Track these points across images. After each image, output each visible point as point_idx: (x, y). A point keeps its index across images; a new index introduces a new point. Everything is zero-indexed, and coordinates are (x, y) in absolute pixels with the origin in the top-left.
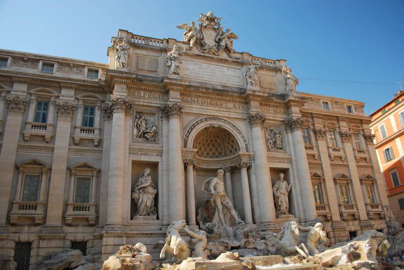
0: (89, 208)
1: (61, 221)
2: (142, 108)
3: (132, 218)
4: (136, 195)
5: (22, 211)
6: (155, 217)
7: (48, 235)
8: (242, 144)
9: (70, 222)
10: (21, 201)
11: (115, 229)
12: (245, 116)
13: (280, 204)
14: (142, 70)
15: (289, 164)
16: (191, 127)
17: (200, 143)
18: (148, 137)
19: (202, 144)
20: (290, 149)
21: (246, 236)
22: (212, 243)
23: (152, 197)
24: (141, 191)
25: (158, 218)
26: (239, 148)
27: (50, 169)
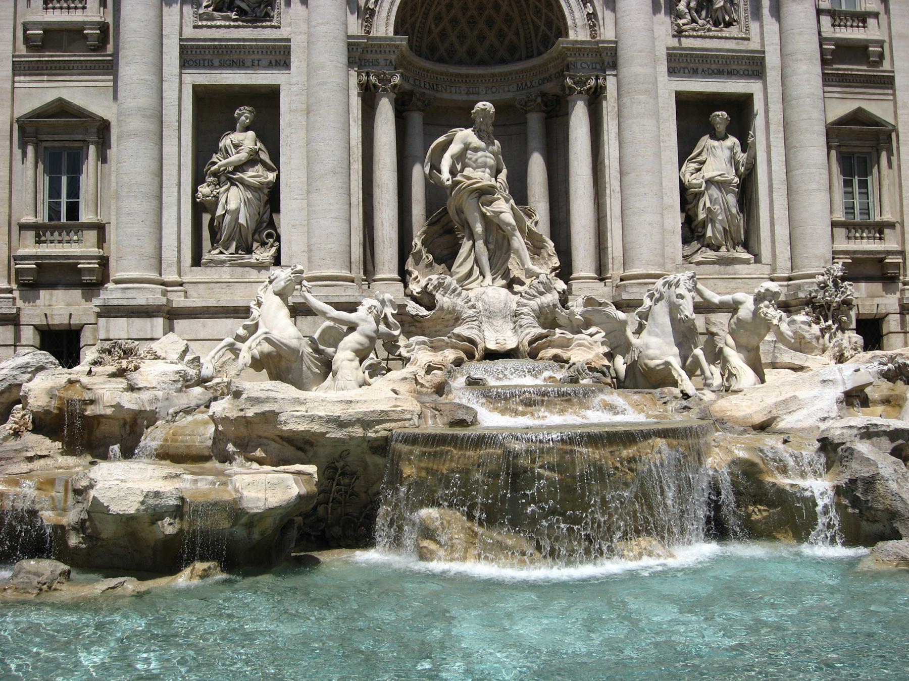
3: (197, 261)
11: (130, 294)
13: (702, 215)
17: (438, 18)
21: (548, 319)
24: (223, 178)
26: (566, 28)
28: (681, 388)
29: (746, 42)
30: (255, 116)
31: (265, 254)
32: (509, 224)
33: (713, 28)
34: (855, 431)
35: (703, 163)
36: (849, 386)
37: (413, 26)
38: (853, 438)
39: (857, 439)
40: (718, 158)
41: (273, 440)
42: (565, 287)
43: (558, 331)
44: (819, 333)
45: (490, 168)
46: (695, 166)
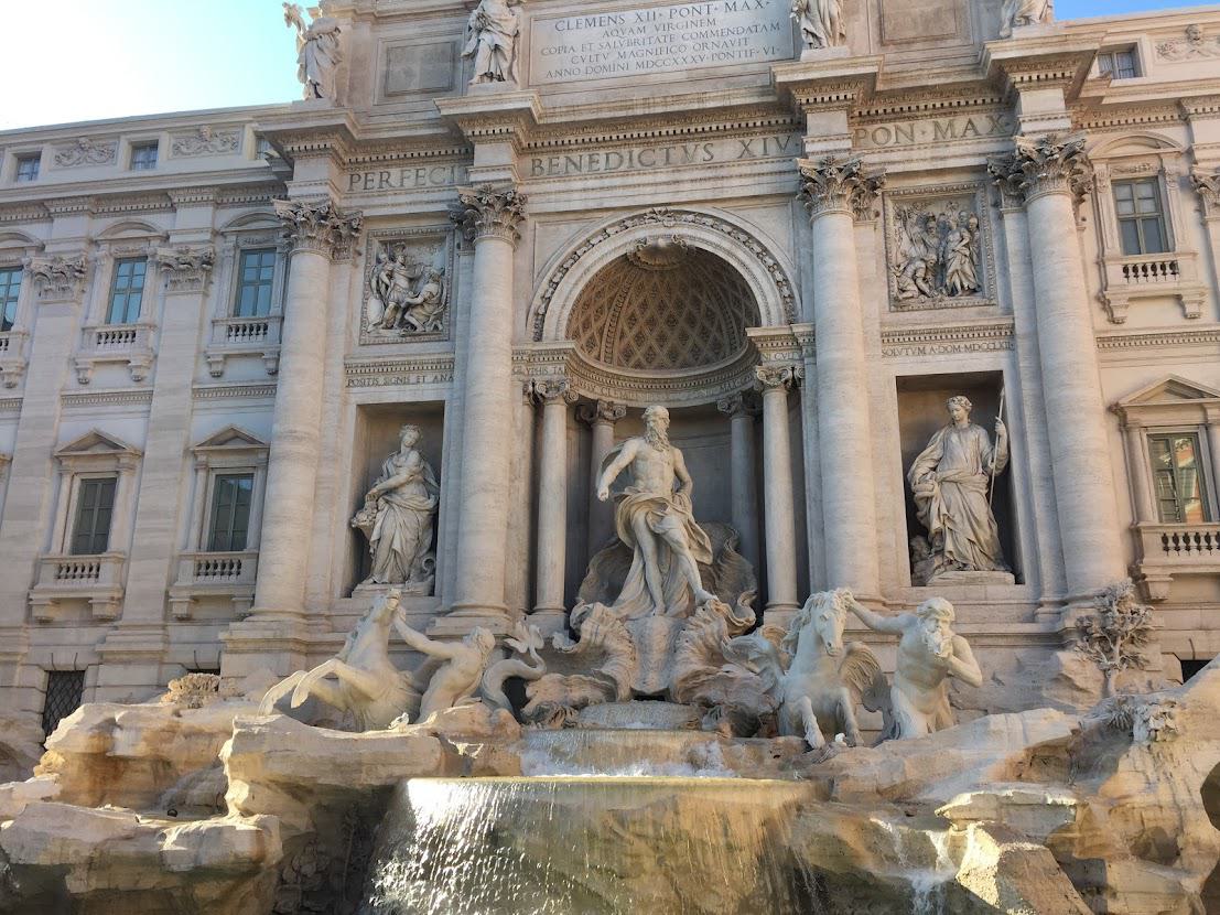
0: (239, 567)
1: (161, 607)
4: (363, 519)
6: (422, 587)
8: (767, 296)
9: (180, 610)
10: (64, 555)
12: (790, 183)
13: (936, 525)
14: (404, 93)
15: (1003, 353)
17: (632, 319)
18: (413, 321)
19: (642, 321)
20: (1007, 287)
22: (558, 676)
24: (381, 502)
25: (432, 593)
28: (807, 738)
29: (991, 308)
31: (419, 584)
32: (677, 542)
33: (947, 298)
41: (268, 786)
42: (752, 617)
43: (726, 667)
44: (1100, 676)
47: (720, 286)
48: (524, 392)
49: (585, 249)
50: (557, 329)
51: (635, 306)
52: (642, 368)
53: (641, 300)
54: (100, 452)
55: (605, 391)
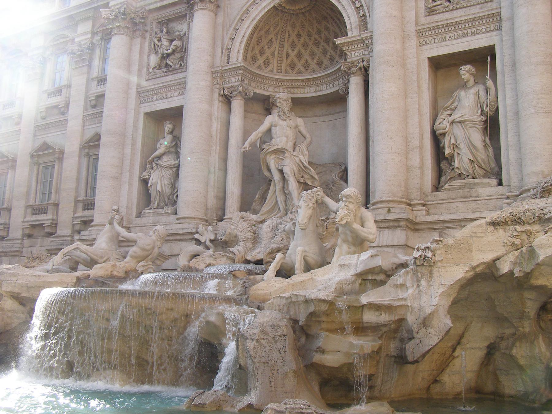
1: (71, 227)
2: (164, 12)
3: (139, 215)
5: (35, 218)
7: (53, 247)
9: (77, 228)
10: (36, 203)
13: (447, 151)
15: (495, 33)
16: (240, 19)
17: (293, 45)
18: (169, 63)
19: (299, 46)
23: (168, 173)
24: (154, 165)
27: (62, 152)
30: (174, 126)
31: (169, 209)
32: (286, 173)
34: (284, 301)
35: (454, 110)
36: (359, 270)
37: (273, 54)
38: (281, 307)
39: (285, 309)
40: (468, 102)
45: (287, 137)
46: (448, 113)
47: (336, 17)
48: (219, 94)
49: (252, 7)
50: (238, 56)
51: (293, 38)
52: (302, 73)
53: (296, 32)
54: (47, 152)
55: (276, 90)
